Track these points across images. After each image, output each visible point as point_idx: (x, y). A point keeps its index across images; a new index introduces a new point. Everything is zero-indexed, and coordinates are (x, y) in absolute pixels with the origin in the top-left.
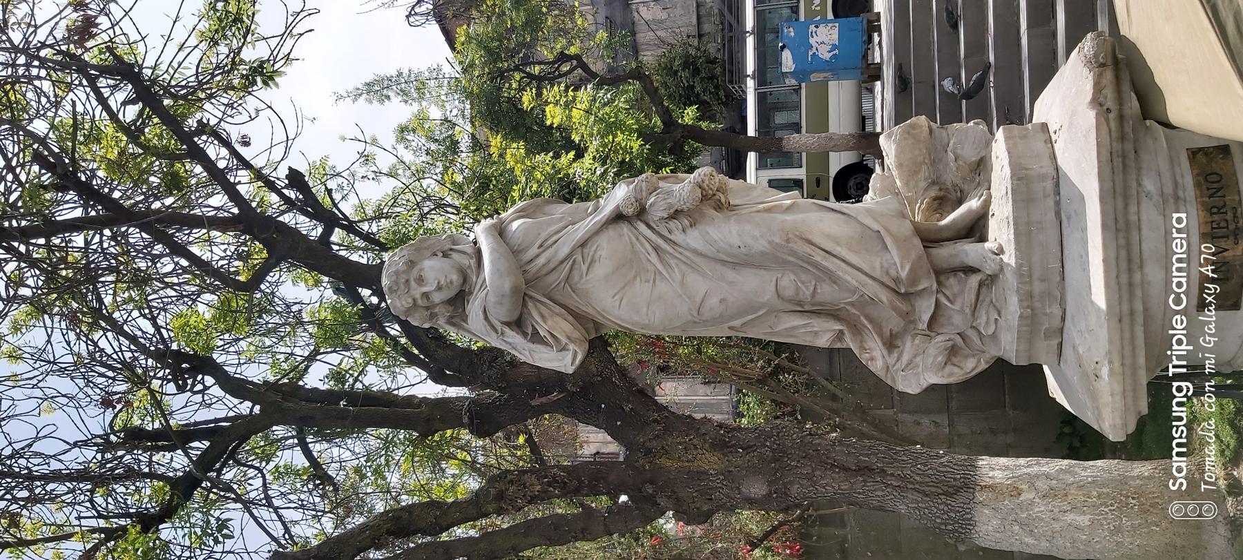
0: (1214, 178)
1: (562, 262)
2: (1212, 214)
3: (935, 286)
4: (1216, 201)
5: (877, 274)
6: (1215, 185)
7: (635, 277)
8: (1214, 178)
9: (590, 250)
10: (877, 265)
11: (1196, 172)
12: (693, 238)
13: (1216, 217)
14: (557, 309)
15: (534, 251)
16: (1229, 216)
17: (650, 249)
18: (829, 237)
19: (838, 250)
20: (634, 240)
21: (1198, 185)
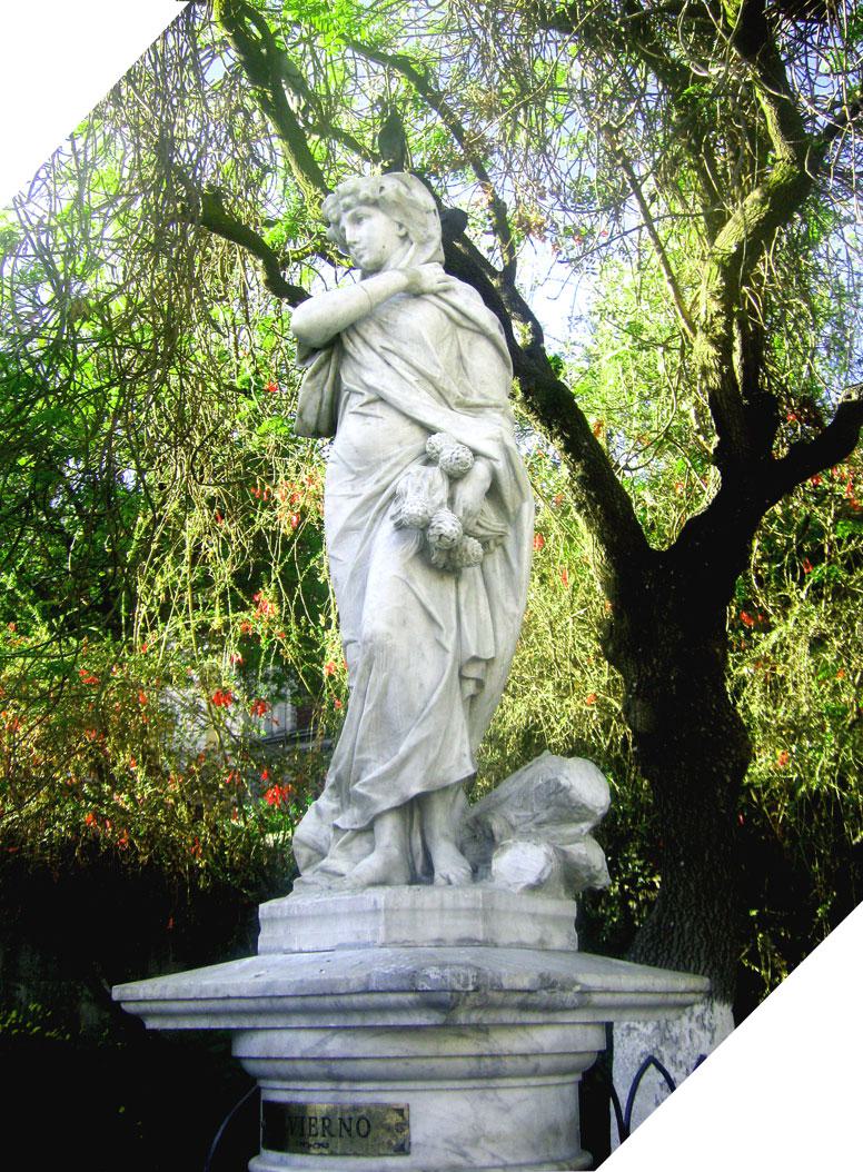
0: (363, 1127)
1: (362, 381)
2: (323, 1119)
3: (357, 826)
4: (336, 1124)
5: (356, 757)
6: (354, 1129)
7: (353, 472)
8: (363, 1127)
9: (378, 409)
10: (364, 756)
11: (373, 1109)
12: (387, 526)
13: (320, 1123)
14: (328, 388)
15: (377, 339)
16: (321, 1139)
17: (384, 482)
18: (384, 694)
19: (368, 708)
20: (393, 461)
21: (356, 1108)
